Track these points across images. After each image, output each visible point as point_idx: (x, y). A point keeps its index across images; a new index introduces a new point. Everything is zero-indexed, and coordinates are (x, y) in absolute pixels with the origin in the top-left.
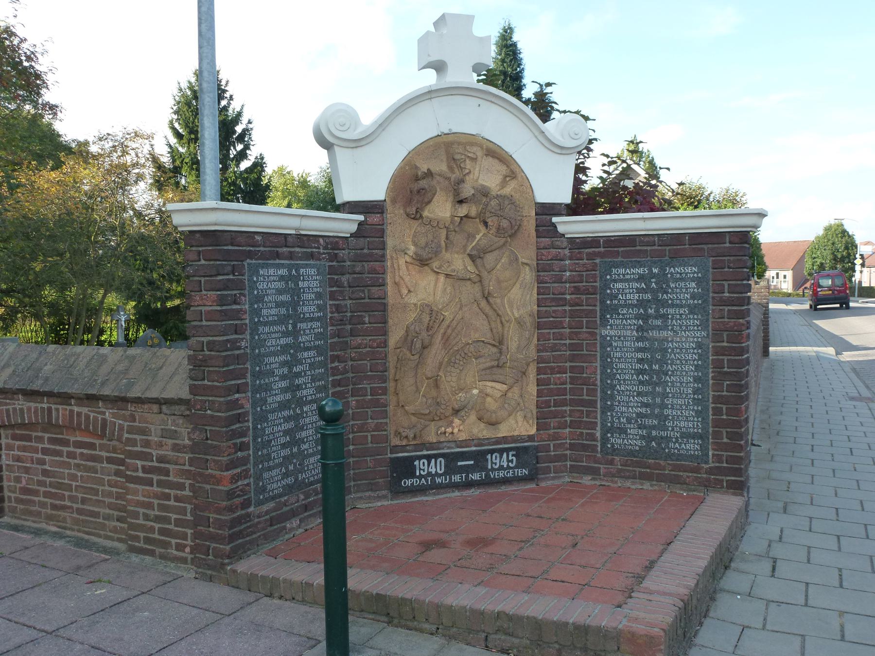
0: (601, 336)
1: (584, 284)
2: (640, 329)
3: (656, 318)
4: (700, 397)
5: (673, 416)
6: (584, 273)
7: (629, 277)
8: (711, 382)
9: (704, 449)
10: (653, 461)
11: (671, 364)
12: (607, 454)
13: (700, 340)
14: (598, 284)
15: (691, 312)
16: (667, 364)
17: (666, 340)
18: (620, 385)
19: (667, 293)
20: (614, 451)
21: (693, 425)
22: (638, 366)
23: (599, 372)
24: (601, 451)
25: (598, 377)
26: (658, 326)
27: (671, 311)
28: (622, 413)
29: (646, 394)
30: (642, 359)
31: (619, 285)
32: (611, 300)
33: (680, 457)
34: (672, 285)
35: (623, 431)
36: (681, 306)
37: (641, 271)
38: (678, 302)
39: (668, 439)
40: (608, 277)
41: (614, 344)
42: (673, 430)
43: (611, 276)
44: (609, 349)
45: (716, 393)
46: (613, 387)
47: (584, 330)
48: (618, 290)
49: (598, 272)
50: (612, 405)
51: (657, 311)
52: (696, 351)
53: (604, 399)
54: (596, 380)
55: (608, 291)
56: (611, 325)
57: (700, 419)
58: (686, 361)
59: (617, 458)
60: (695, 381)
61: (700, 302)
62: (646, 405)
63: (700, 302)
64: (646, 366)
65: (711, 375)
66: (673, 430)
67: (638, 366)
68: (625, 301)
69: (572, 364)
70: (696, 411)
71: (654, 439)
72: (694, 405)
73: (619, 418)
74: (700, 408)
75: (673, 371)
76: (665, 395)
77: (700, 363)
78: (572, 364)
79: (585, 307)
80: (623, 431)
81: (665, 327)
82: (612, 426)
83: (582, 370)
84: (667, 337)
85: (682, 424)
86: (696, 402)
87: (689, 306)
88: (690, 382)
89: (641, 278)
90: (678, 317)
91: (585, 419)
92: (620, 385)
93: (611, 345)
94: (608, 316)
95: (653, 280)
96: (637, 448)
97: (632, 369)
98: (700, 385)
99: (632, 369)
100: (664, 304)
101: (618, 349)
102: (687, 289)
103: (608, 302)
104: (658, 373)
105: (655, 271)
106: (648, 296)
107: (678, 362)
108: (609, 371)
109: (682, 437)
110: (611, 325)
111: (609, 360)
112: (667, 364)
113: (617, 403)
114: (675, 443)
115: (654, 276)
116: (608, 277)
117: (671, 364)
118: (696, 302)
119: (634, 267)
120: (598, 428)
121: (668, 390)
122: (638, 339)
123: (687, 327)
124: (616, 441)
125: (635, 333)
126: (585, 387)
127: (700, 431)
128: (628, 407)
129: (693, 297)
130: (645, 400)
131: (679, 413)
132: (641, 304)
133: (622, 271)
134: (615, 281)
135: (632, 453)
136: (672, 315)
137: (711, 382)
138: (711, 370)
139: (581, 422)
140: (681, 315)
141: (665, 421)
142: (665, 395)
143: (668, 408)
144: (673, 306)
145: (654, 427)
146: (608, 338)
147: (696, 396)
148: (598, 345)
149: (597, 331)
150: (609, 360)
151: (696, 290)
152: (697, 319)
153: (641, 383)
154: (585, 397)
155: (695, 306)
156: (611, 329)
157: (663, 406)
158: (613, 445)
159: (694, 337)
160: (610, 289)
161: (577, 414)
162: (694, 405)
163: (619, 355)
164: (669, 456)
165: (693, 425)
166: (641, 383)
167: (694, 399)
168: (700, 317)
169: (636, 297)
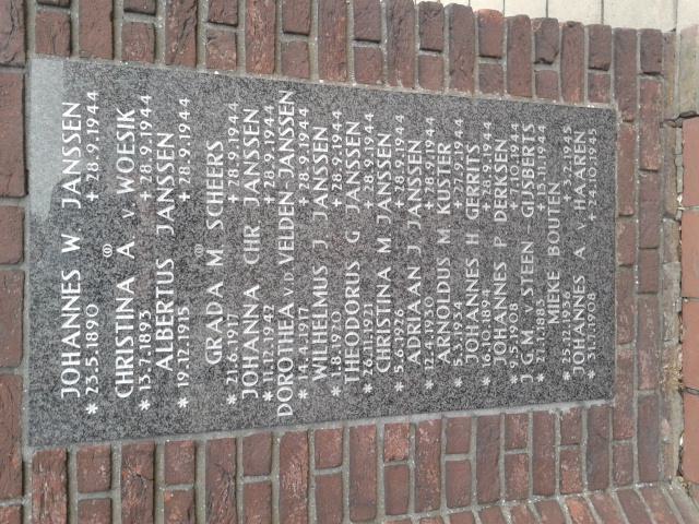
0: (297, 418)
1: (116, 495)
2: (270, 295)
3: (237, 242)
4: (459, 122)
5: (512, 198)
6: (77, 497)
7: (92, 338)
8: (419, 90)
9: (584, 120)
10: (618, 255)
11: (376, 199)
12: (610, 379)
13: (304, 111)
14: (118, 446)
15: (220, 132)
16: (376, 211)
17: (302, 214)
18: (437, 350)
19: (154, 206)
20: (602, 360)
21: (528, 143)
22: (383, 296)
23: (401, 419)
24: (605, 396)
25: (417, 418)
26: (264, 236)
27: (214, 196)
28: (510, 342)
29: (458, 272)
30: (364, 285)
31: (124, 368)
32: (177, 393)
33: (605, 185)
34: (127, 186)
35: (553, 339)
36: (200, 160)
37: (72, 295)
38: (184, 170)
39: (566, 214)
40: (92, 409)
41: (320, 374)
42: (543, 200)
43: (86, 401)
44: (336, 392)
45: (448, 80)
46: (445, 372)
47: (275, 477)
48: (139, 371)
49: (74, 449)
50: (491, 372)
51: (215, 239)
52: (337, 126)
53: (478, 399)
54: (425, 424)
55: (145, 405)
56: (262, 389)
57: (515, 126)
58: (366, 155)
59: (619, 351)
60: (418, 134)
61: (184, 102)
62: (487, 271)
63: (184, 102)
64: (383, 274)
65: (401, 88)
66: (543, 200)
67: (383, 296)
68: (178, 344)
69: (382, 507)
70: (497, 134)
71: (568, 253)
72: (479, 140)
73: (523, 350)
74: (487, 125)
75: (395, 195)
76: (458, 220)
77: (369, 116)
78: (382, 507)
79: (201, 484)
80: (553, 339)
81: (267, 215)
82: (544, 369)
83: (396, 471)
84: (299, 209)
85: (527, 174)
86: (472, 134)
87: (198, 136)
88: (422, 147)
89: (98, 292)
90: (233, 173)
91: (529, 452)
92: (437, 350)
93: (323, 385)
94: (232, 400)
95: (107, 251)
96: (592, 296)
97: (391, 316)
98: (429, 120)
99: (391, 316)
100: (190, 219)
101: (336, 360)
102: (140, 141)
103: (183, 403)
104: (400, 241)
105: (72, 243)
106: (164, 267)
107: (368, 178)
108: (399, 387)
109: (560, 177)
110: (262, 389)
111: (368, 389)
112: (376, 211)
113: (486, 358)
114: (574, 196)
115: (91, 250)
116: (92, 409)
117: (376, 199)
118: (184, 115)
119: (57, 317)
120: (550, 408)
121: (444, 210)
122: (304, 299)
123: (264, 149)
124: (578, 355)
125: (285, 310)
126: (446, 458)
127: (542, 128)
128: (495, 324)
129: (170, 123)
130: (473, 276)
131: (501, 182)
132: (190, 281)
133: (69, 362)
134: (107, 383)
135: (605, 313)
136: (227, 190)
137: (419, 90)
138: (388, 87)
139: (536, 459)
140: (227, 164)
141: (523, 221)
142: (458, 220)
143: (492, 211)
144: (198, 191)
145: (540, 252)
146: (303, 395)
147: (459, 134)
148: (324, 427)
149: (281, 432)
150: (368, 389)
151: (145, 112)
152: (242, 115)
153: (428, 287)
154: (472, 457)
155: (198, 116)
156: (274, 387)
157: (486, 226)
158: (589, 365)
159: (297, 130)
160: (135, 400)
161: (520, 472)
162: (479, 140)
163: (352, 358)
164: (604, 209)
165: (528, 143)
166: (428, 287)
167: (465, 139)
168: (234, 106)
169: (168, 308)
